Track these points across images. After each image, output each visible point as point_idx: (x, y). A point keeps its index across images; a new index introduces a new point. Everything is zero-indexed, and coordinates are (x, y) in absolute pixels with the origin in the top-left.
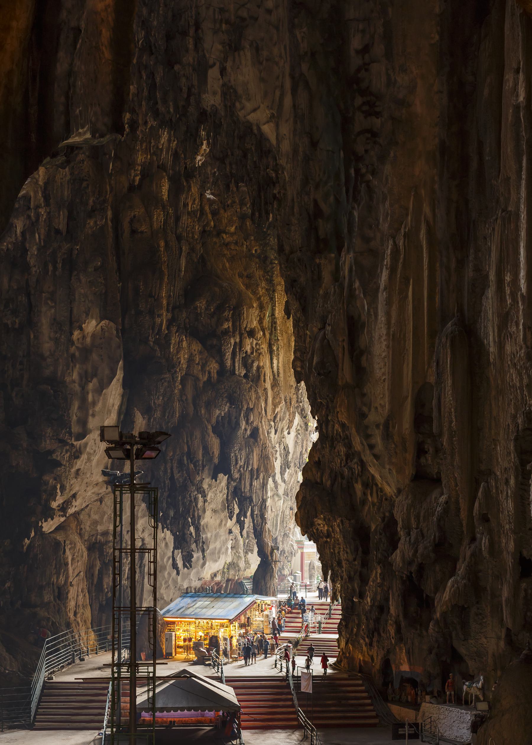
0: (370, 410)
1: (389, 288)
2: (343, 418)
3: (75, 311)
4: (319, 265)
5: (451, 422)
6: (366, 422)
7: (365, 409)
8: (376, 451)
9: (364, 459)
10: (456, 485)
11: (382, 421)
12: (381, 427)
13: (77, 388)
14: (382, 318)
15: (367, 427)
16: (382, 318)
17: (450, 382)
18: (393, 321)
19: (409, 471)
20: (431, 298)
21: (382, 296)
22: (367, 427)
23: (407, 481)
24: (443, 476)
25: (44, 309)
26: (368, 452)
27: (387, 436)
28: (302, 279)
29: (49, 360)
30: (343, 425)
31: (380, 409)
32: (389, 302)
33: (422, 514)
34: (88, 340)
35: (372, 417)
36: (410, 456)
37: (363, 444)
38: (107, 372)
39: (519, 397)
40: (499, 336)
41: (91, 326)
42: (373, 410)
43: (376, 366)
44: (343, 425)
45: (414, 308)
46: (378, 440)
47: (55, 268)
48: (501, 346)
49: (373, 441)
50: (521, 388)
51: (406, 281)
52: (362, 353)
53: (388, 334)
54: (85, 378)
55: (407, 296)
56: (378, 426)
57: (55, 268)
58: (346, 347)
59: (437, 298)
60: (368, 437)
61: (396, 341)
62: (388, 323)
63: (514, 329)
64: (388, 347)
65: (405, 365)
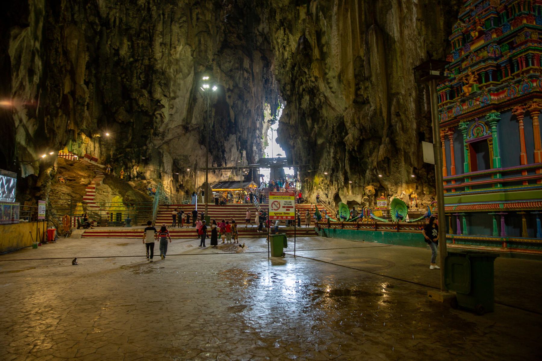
0: (329, 70)
1: (338, 14)
2: (316, 73)
3: (173, 40)
4: (298, 10)
5: (377, 70)
6: (327, 76)
7: (327, 71)
8: (333, 90)
9: (326, 94)
10: (380, 101)
11: (337, 74)
12: (337, 77)
13: (173, 76)
14: (334, 28)
15: (328, 79)
16: (334, 28)
17: (376, 50)
18: (341, 28)
19: (352, 97)
20: (360, 17)
21: (334, 18)
22: (328, 79)
23: (351, 102)
24: (370, 99)
25: (157, 38)
26: (329, 90)
27: (340, 81)
28: (290, 17)
29: (159, 61)
30: (316, 78)
31: (335, 68)
32: (338, 20)
33: (361, 117)
34: (178, 56)
35: (331, 74)
36: (352, 90)
37: (325, 87)
38: (186, 71)
39: (415, 54)
40: (401, 28)
41: (180, 48)
42: (331, 69)
43: (333, 50)
44: (316, 78)
45: (352, 22)
46: (334, 84)
47: (164, 18)
48: (401, 32)
49: (331, 85)
50: (416, 49)
51: (347, 10)
52: (323, 45)
53: (338, 34)
54: (177, 72)
55: (347, 17)
56: (334, 77)
57: (164, 18)
58: (316, 42)
59: (363, 17)
60: (328, 83)
61: (343, 37)
62: (338, 29)
63: (409, 22)
64: (338, 40)
65: (348, 48)
